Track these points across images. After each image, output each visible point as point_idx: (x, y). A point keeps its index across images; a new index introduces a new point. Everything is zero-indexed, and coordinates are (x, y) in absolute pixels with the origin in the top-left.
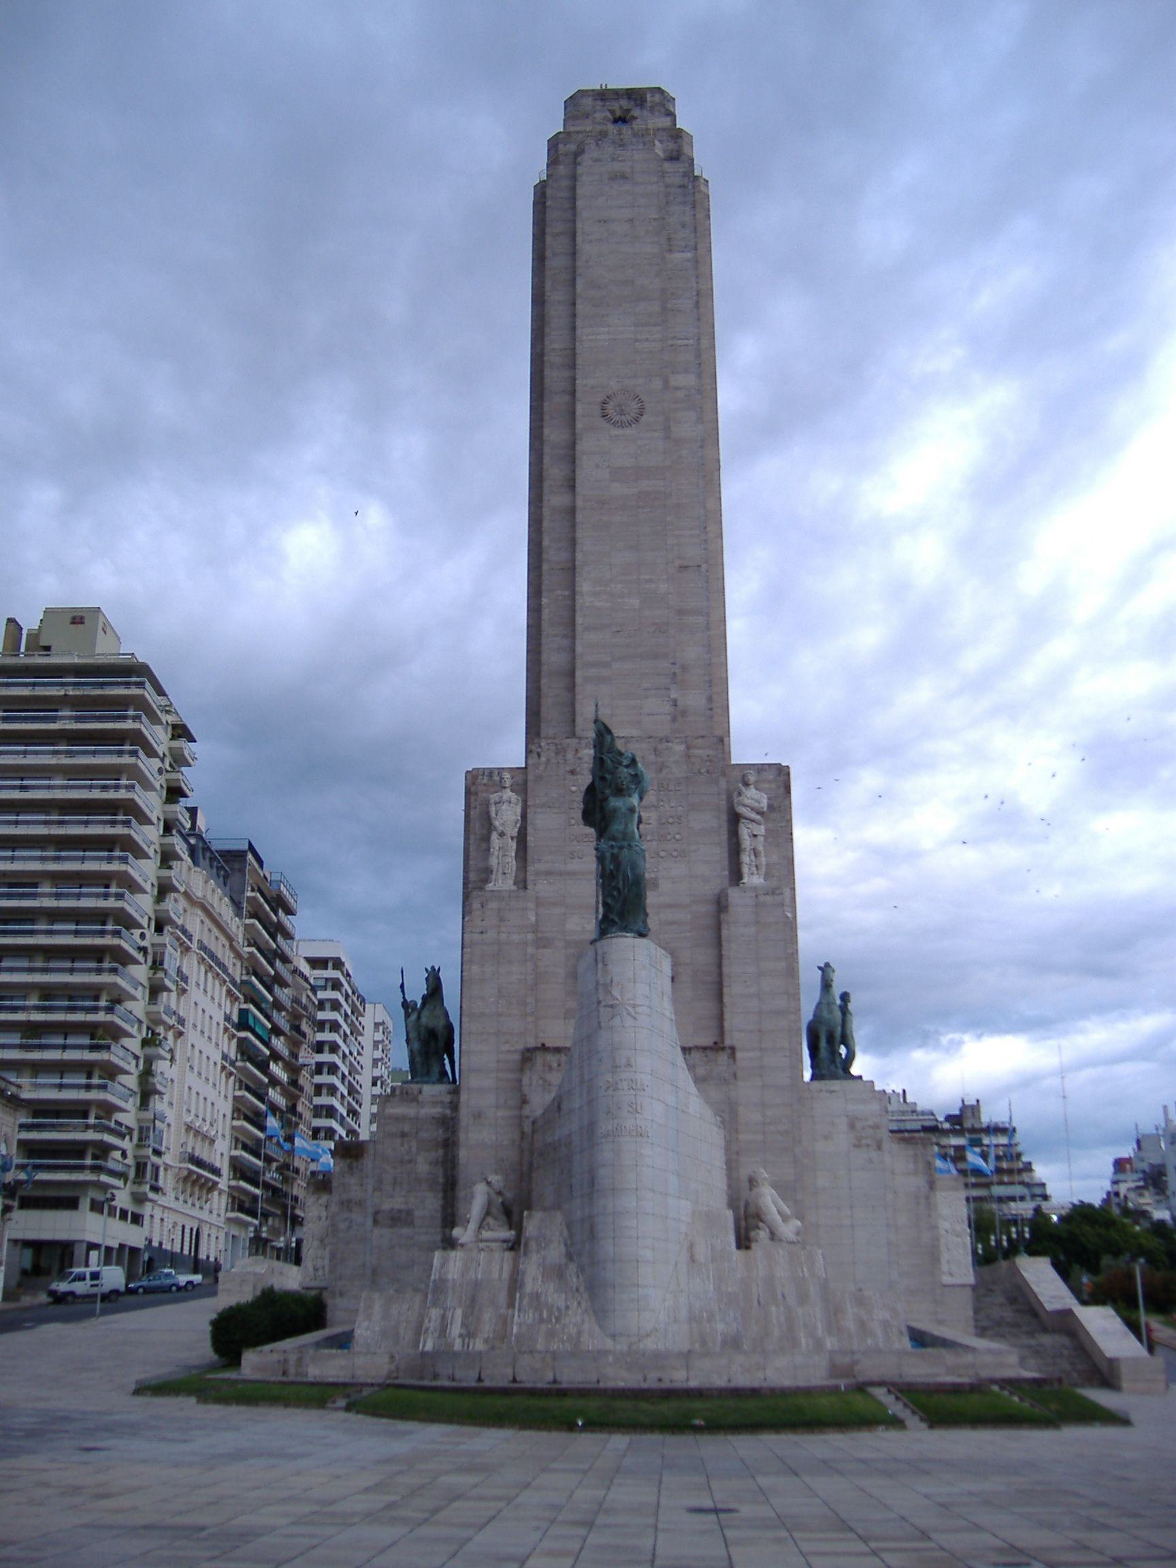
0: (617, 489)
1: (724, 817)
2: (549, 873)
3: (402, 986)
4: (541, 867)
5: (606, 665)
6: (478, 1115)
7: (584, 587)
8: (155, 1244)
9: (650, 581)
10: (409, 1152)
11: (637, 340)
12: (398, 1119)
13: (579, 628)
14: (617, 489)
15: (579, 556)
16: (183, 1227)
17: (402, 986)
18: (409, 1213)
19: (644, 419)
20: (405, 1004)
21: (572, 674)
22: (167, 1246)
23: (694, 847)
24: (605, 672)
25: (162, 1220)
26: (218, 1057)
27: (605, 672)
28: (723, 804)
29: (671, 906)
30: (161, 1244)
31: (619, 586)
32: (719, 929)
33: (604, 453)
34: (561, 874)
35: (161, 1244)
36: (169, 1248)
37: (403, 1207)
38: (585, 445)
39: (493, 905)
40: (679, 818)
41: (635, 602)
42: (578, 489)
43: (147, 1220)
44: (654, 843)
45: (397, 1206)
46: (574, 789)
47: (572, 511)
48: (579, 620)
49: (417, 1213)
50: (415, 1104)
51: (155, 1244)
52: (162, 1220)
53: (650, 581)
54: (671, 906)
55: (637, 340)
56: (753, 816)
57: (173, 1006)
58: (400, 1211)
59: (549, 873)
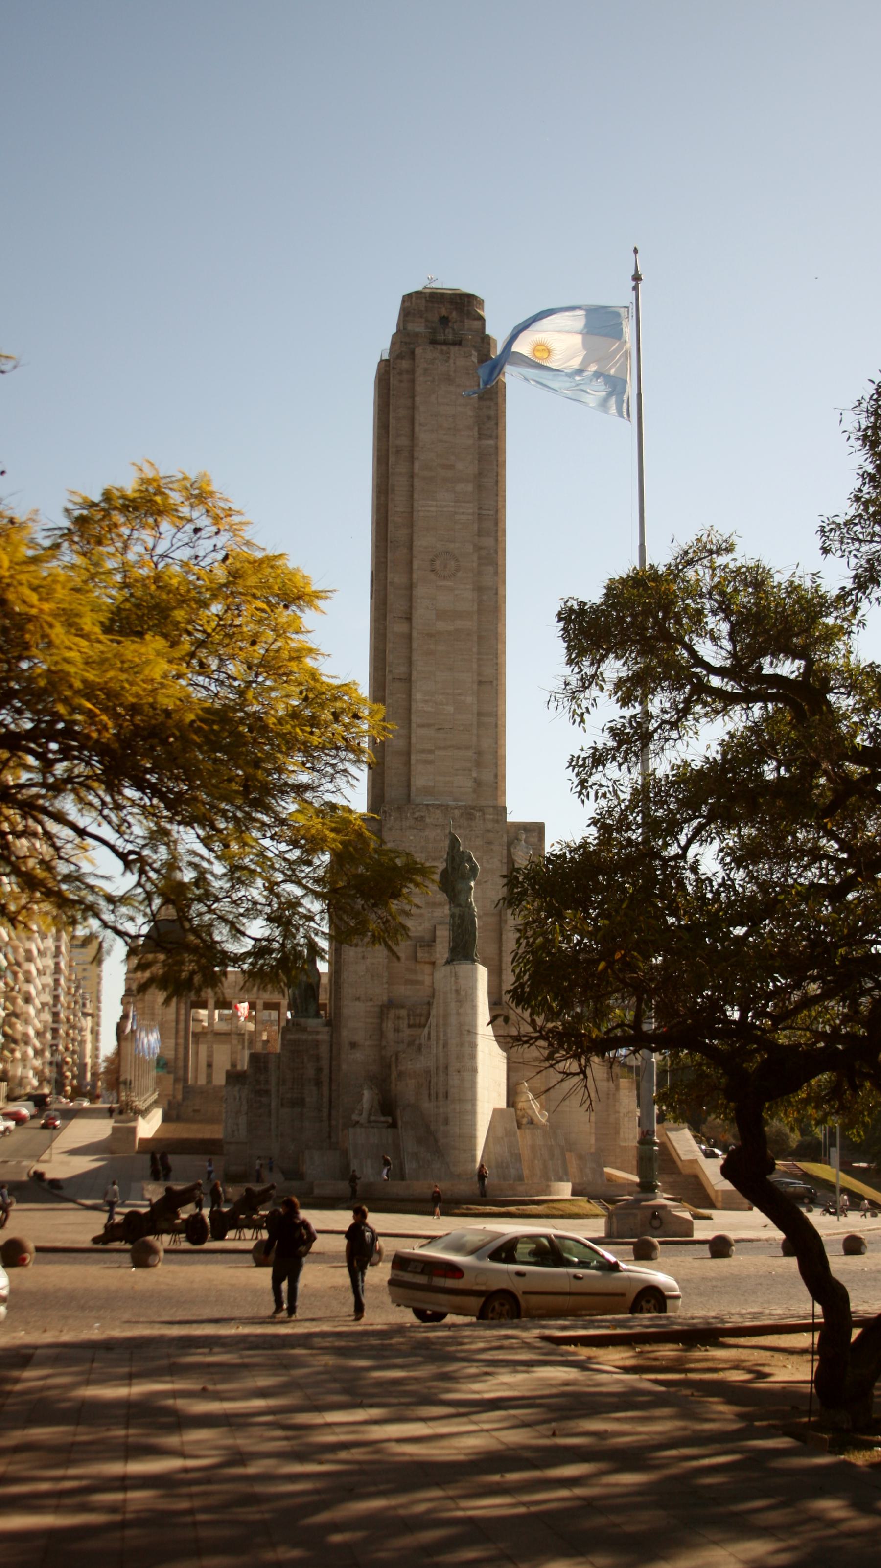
0: (441, 626)
1: (505, 861)
5: (431, 752)
6: (353, 1045)
7: (418, 696)
9: (460, 694)
11: (456, 513)
13: (414, 725)
14: (441, 626)
15: (414, 673)
19: (459, 574)
21: (409, 754)
24: (430, 757)
27: (430, 757)
32: (501, 935)
33: (433, 599)
38: (420, 591)
41: (450, 709)
42: (414, 620)
47: (409, 637)
48: (414, 718)
49: (308, 1100)
55: (456, 513)
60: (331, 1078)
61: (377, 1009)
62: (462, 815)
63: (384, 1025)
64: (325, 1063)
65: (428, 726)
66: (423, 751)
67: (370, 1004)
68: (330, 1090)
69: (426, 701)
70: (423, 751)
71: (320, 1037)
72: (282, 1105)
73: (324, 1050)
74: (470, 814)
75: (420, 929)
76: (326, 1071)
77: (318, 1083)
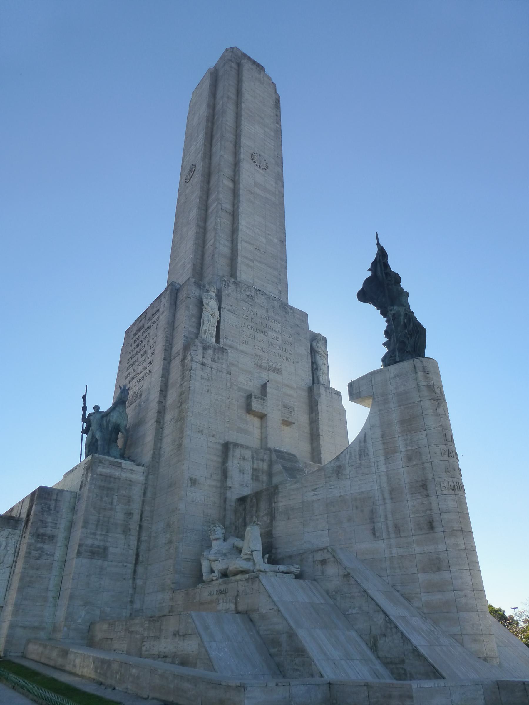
2: (231, 347)
3: (84, 397)
4: (229, 342)
6: (193, 482)
9: (269, 235)
10: (112, 503)
12: (107, 477)
17: (84, 397)
18: (105, 549)
20: (84, 408)
23: (297, 361)
24: (251, 264)
27: (251, 264)
28: (309, 345)
29: (288, 386)
31: (257, 230)
34: (237, 349)
37: (102, 543)
39: (210, 352)
40: (291, 343)
44: (280, 351)
45: (96, 543)
46: (244, 308)
49: (111, 550)
50: (120, 469)
53: (269, 235)
54: (288, 386)
56: (323, 353)
58: (98, 547)
59: (231, 347)
60: (140, 527)
61: (220, 447)
62: (280, 306)
63: (230, 463)
64: (136, 507)
65: (250, 243)
66: (246, 258)
67: (212, 439)
68: (139, 540)
69: (249, 228)
70: (246, 258)
71: (134, 477)
72: (79, 553)
73: (137, 492)
74: (286, 309)
75: (251, 384)
76: (136, 517)
77: (126, 531)
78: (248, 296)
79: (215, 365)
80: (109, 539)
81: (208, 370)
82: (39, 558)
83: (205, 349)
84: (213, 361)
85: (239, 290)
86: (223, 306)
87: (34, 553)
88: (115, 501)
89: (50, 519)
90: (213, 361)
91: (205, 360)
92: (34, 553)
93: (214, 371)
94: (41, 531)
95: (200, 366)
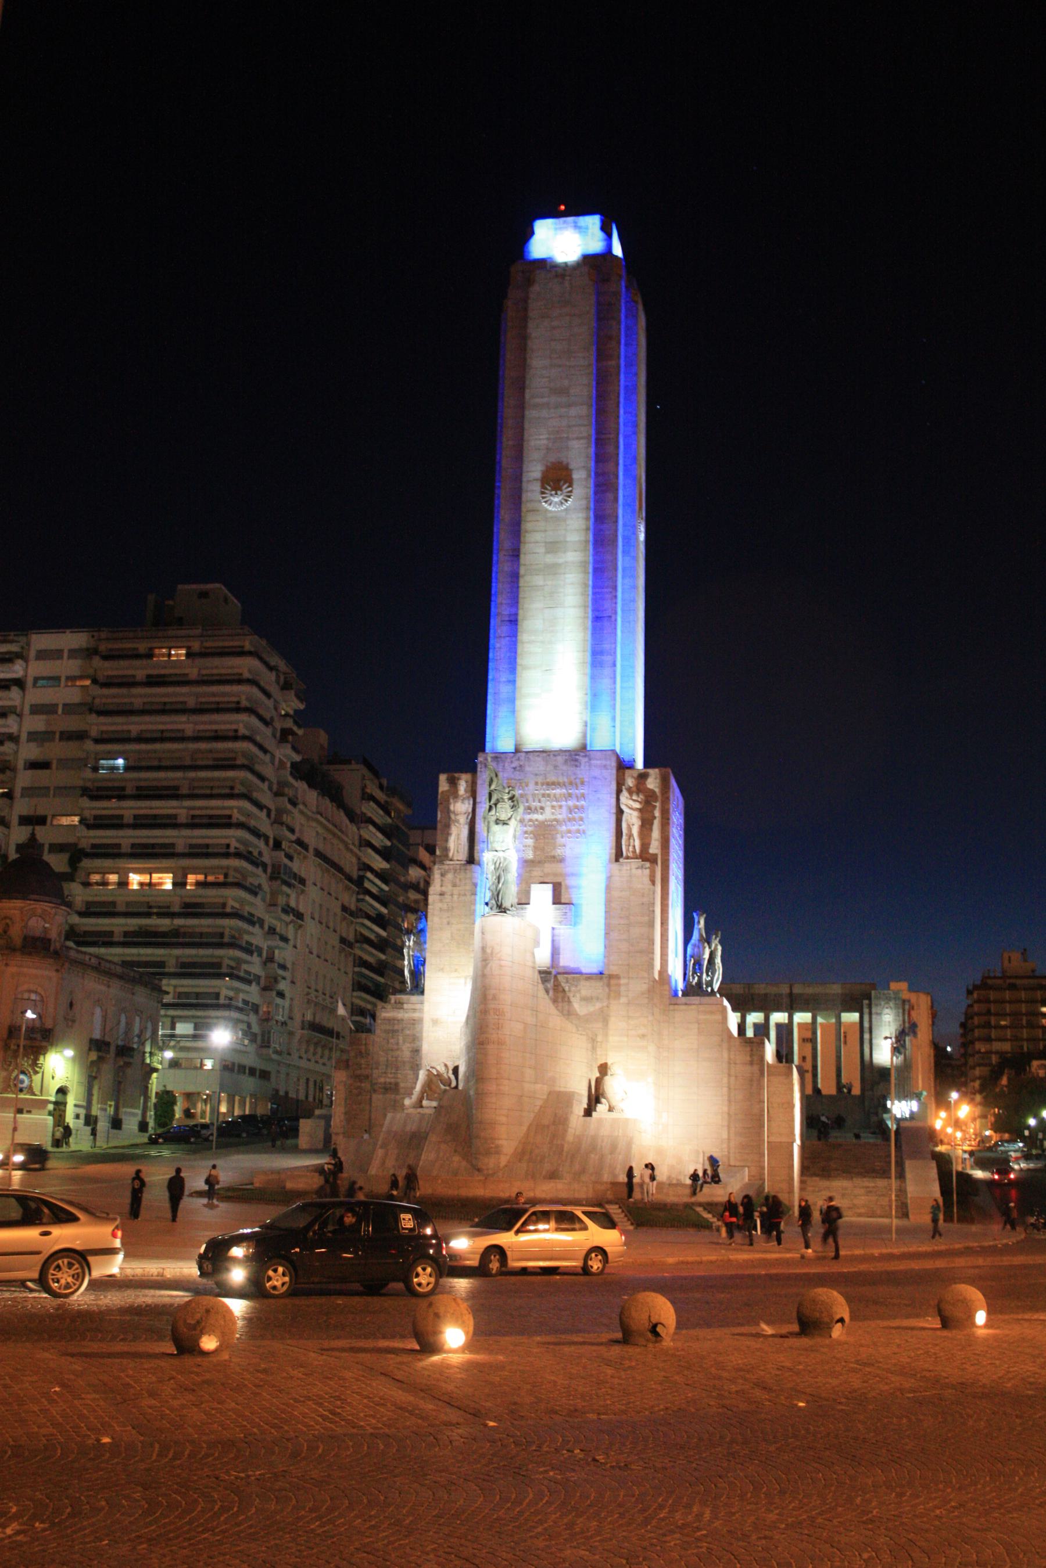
8: (282, 1093)
10: (398, 1044)
16: (308, 1080)
18: (397, 1084)
22: (292, 1095)
25: (288, 1074)
26: (336, 942)
30: (287, 1093)
35: (287, 1093)
36: (294, 1096)
37: (393, 1080)
39: (450, 876)
43: (273, 1076)
45: (388, 1080)
49: (402, 1085)
51: (282, 1093)
52: (288, 1074)
57: (293, 904)
58: (390, 1083)
62: (566, 761)
74: (576, 760)
78: (514, 768)
79: (456, 891)
80: (399, 1076)
81: (448, 897)
82: (360, 1094)
83: (442, 875)
84: (454, 885)
85: (501, 764)
86: (478, 800)
87: (355, 1091)
88: (401, 1041)
89: (363, 1061)
90: (454, 885)
91: (444, 889)
92: (355, 1091)
93: (455, 897)
94: (358, 1072)
95: (438, 897)
